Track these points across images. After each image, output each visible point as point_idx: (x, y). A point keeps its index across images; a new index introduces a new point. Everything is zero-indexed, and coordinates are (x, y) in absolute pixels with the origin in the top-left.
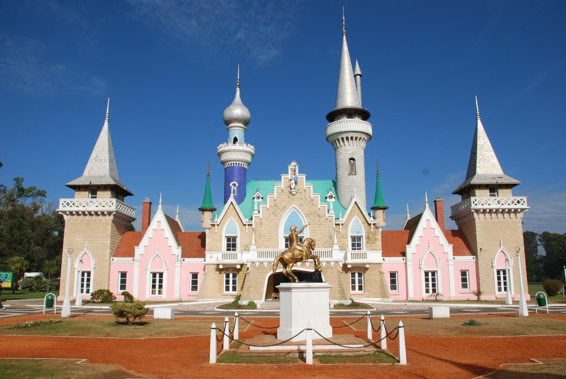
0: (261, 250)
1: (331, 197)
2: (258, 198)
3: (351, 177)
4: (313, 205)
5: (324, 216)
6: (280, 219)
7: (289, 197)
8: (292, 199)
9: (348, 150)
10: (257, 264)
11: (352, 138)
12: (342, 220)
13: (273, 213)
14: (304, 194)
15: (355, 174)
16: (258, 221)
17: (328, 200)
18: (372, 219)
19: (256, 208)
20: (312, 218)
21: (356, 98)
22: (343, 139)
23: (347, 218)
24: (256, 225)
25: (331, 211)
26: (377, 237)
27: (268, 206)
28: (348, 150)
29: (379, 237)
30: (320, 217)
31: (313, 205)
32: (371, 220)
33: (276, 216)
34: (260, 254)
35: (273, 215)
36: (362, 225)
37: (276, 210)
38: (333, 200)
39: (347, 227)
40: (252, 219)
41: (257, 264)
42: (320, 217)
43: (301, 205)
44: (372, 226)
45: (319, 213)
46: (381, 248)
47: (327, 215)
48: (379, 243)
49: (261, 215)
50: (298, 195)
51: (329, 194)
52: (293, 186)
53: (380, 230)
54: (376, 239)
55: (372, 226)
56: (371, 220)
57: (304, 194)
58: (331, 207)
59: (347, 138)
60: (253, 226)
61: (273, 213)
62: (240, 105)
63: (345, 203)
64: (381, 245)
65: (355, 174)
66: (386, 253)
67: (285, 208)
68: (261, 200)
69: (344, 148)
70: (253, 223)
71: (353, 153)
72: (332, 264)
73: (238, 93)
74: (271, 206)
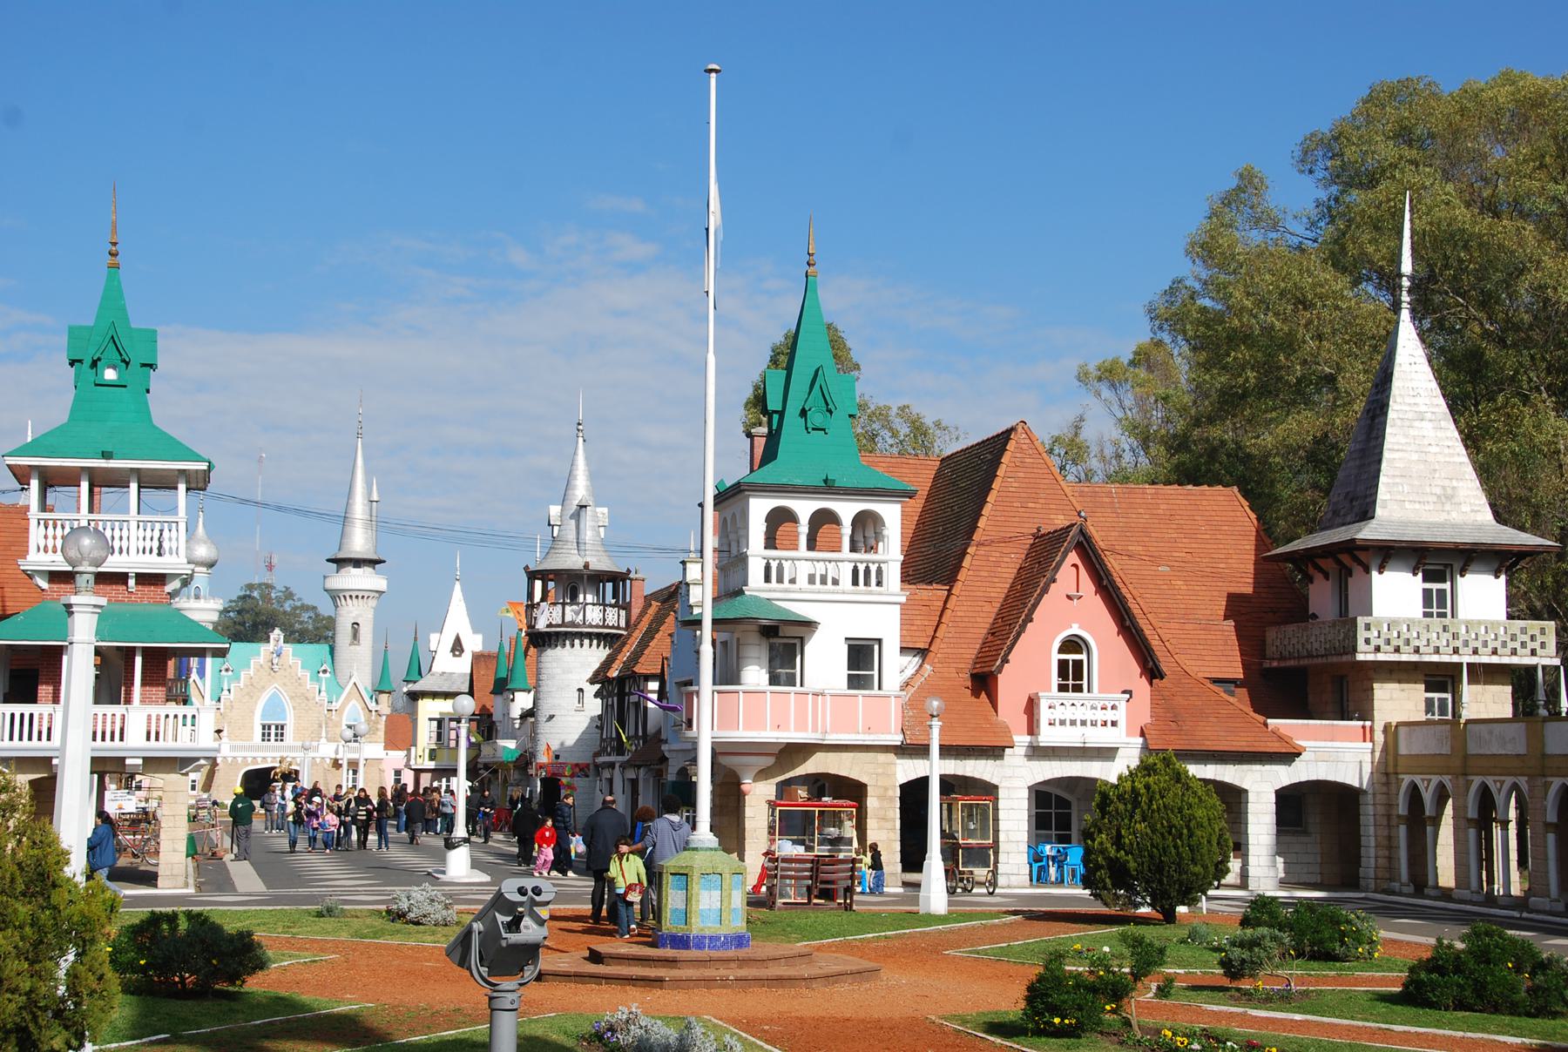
0: (235, 743)
1: (325, 671)
2: (227, 670)
3: (353, 647)
4: (300, 685)
5: (314, 698)
6: (256, 703)
7: (270, 674)
8: (273, 677)
9: (351, 612)
10: (230, 760)
11: (357, 597)
12: (335, 706)
13: (248, 694)
14: (289, 670)
15: (359, 644)
16: (228, 704)
17: (321, 674)
18: (374, 704)
19: (226, 687)
20: (298, 701)
21: (367, 539)
22: (345, 597)
23: (343, 703)
24: (225, 709)
25: (323, 694)
26: (379, 726)
27: (242, 685)
28: (351, 612)
29: (382, 726)
30: (308, 700)
31: (300, 685)
32: (372, 706)
33: (252, 697)
34: (233, 748)
35: (247, 697)
36: (361, 711)
37: (253, 689)
38: (328, 675)
39: (342, 713)
40: (219, 700)
41: (230, 760)
42: (308, 700)
43: (285, 684)
44: (374, 713)
45: (307, 695)
46: (383, 740)
47: (317, 699)
48: (381, 734)
49: (232, 696)
50: (282, 672)
51: (323, 668)
52: (275, 661)
53: (384, 718)
54: (377, 729)
55: (374, 713)
56: (372, 706)
57: (289, 670)
58: (323, 688)
59: (351, 597)
60: (222, 711)
61: (248, 694)
62: (205, 543)
63: (342, 681)
64: (383, 736)
65: (359, 644)
66: (391, 744)
67: (263, 687)
68: (230, 673)
69: (345, 608)
70: (222, 707)
71: (358, 616)
72: (318, 760)
73: (201, 520)
74: (246, 686)
